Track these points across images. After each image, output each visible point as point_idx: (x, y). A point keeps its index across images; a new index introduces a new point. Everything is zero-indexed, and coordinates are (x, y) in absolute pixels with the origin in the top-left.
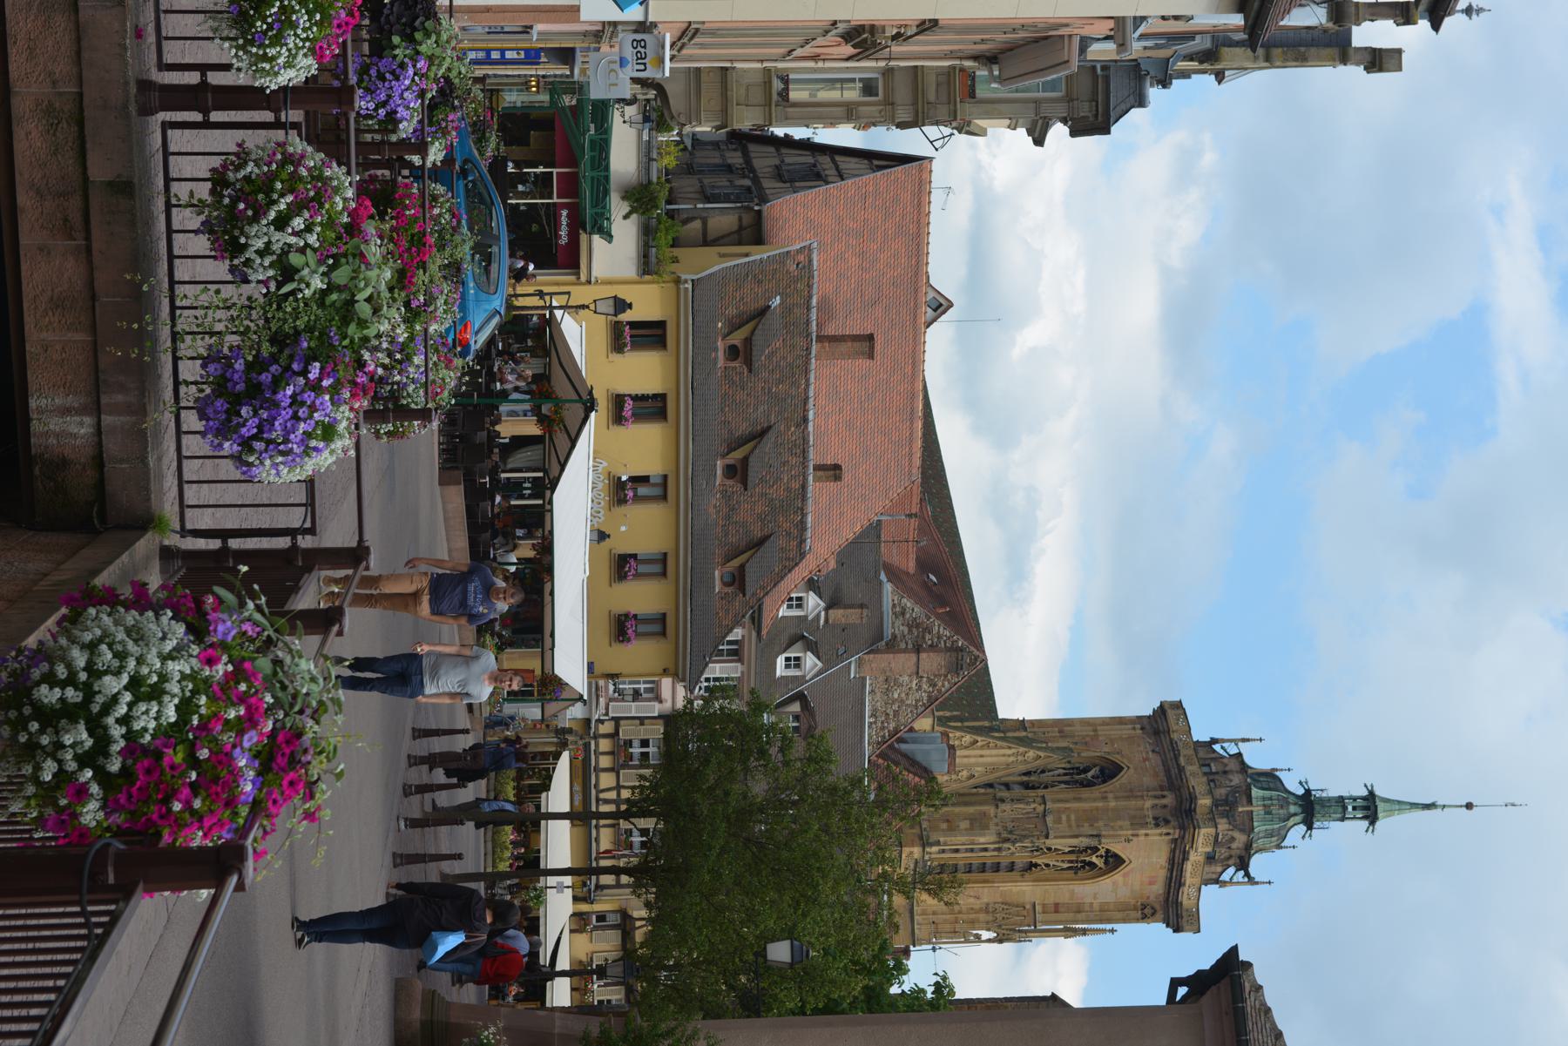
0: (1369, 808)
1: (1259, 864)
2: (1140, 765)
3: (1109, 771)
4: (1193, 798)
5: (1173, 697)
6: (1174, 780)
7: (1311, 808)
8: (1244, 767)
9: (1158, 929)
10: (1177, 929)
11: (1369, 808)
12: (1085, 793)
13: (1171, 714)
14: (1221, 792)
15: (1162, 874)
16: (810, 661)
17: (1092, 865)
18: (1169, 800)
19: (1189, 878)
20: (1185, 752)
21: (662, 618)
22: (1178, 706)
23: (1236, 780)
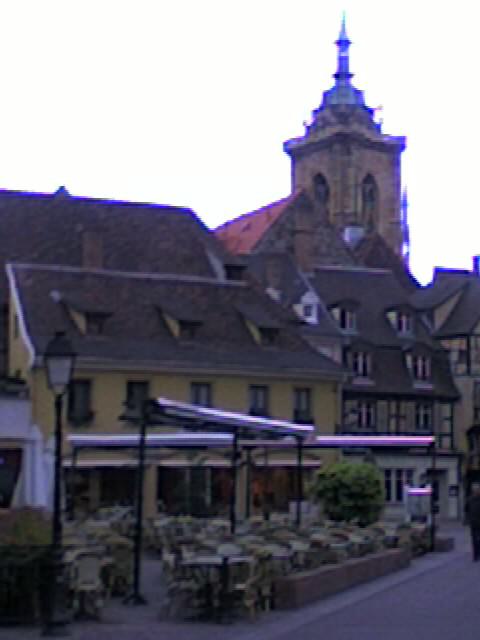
0: (343, 43)
1: (369, 103)
2: (318, 163)
3: (320, 179)
4: (338, 135)
5: (281, 147)
6: (326, 145)
7: (343, 75)
8: (322, 108)
9: (404, 156)
10: (403, 147)
11: (343, 43)
12: (332, 191)
13: (289, 147)
14: (333, 119)
15: (377, 154)
16: (310, 298)
17: (371, 191)
18: (337, 147)
19: (375, 139)
20: (312, 139)
21: (298, 391)
22: (286, 144)
23: (327, 112)
